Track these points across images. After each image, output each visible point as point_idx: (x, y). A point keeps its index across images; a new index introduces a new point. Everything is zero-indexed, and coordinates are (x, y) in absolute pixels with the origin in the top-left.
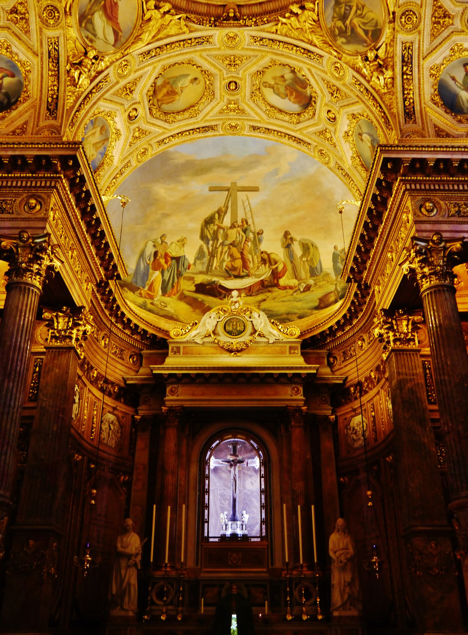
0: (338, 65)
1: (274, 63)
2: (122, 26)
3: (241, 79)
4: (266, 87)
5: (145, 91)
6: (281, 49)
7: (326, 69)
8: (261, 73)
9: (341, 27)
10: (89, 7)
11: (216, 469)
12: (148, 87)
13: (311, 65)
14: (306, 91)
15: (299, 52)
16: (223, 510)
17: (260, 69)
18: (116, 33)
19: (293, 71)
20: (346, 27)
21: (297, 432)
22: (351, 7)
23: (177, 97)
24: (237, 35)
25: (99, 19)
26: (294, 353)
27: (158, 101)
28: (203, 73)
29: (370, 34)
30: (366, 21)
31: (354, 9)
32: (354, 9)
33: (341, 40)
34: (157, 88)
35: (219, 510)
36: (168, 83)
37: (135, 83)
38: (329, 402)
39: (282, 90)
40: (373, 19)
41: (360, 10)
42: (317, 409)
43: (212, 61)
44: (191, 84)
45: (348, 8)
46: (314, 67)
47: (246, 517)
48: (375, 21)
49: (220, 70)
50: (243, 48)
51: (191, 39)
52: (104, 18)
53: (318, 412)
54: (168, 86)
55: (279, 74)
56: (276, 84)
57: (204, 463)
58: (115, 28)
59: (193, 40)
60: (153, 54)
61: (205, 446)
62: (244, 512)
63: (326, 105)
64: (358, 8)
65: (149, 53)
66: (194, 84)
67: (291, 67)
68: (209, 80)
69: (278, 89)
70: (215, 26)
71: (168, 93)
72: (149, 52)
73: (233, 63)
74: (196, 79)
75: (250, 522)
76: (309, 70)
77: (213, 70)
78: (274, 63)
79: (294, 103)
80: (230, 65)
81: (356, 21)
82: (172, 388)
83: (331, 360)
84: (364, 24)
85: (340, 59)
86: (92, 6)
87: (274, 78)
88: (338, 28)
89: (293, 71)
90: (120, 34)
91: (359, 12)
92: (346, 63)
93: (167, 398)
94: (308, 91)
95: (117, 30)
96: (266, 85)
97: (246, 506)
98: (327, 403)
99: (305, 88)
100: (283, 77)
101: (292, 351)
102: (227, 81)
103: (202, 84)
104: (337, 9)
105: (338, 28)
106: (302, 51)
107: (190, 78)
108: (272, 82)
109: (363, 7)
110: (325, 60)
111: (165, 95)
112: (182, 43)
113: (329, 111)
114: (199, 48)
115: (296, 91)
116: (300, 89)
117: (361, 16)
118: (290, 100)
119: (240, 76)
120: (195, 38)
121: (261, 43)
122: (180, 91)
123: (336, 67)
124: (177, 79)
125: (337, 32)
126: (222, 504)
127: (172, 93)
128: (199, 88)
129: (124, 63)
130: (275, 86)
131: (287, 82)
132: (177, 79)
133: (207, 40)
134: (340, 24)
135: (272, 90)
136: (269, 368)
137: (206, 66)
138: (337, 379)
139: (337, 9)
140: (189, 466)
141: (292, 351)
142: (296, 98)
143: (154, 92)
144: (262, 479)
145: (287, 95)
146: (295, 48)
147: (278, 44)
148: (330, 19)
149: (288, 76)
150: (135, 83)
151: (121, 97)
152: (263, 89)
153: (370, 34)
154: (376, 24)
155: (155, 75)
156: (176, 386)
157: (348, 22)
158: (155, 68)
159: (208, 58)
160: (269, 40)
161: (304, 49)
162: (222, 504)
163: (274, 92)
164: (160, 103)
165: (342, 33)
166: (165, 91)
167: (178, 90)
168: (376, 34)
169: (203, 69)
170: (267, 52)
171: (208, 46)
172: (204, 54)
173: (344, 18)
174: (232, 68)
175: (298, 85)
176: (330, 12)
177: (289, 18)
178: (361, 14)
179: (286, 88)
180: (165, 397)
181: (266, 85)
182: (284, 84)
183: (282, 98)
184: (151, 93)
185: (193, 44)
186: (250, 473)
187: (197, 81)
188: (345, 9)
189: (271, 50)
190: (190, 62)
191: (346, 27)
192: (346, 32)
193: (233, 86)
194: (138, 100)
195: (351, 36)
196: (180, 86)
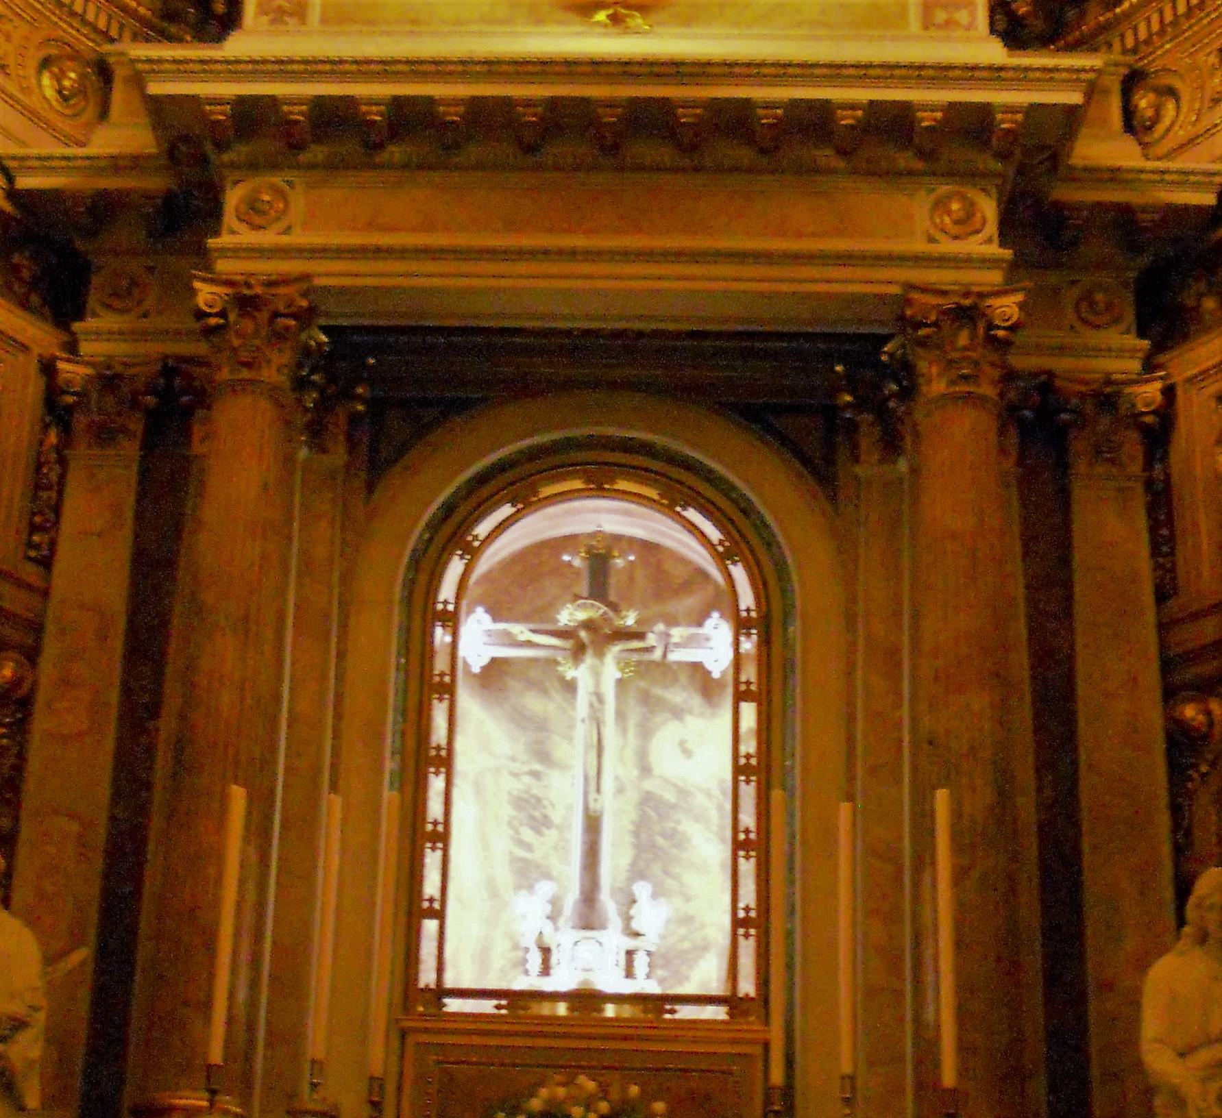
11: (494, 675)
16: (527, 873)
21: (956, 454)
26: (948, 24)
35: (505, 876)
38: (1130, 316)
42: (1062, 350)
47: (652, 916)
53: (1062, 364)
57: (423, 614)
61: (434, 526)
62: (642, 890)
75: (673, 935)
82: (257, 191)
83: (1144, 102)
93: (225, 240)
97: (655, 851)
98: (1117, 320)
101: (941, 16)
126: (520, 843)
136: (805, 71)
138: (1185, 179)
140: (344, 627)
141: (941, 16)
144: (749, 712)
156: (277, 180)
162: (520, 843)
180: (217, 233)
186: (677, 695)
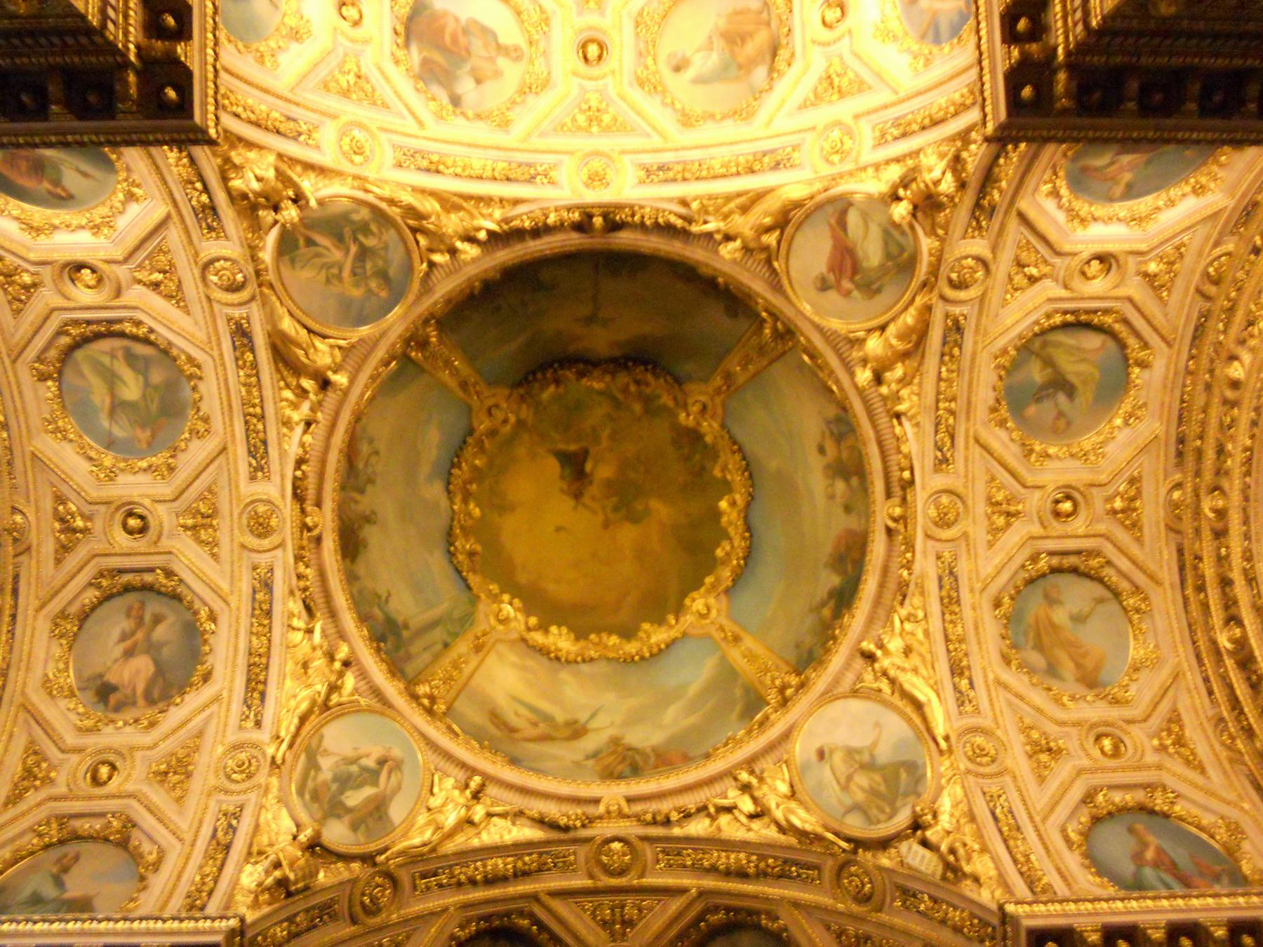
0: (358, 159)
1: (505, 124)
2: (827, 233)
3: (575, 74)
4: (517, 48)
5: (798, 65)
6: (489, 163)
7: (383, 137)
8: (526, 90)
9: (366, 236)
10: (887, 278)
12: (791, 75)
13: (416, 137)
14: (420, 52)
15: (450, 162)
17: (531, 99)
18: (842, 223)
19: (456, 101)
20: (355, 240)
22: (354, 274)
23: (722, 23)
24: (587, 186)
25: (872, 253)
27: (768, 24)
28: (659, 89)
29: (302, 242)
30: (317, 260)
31: (346, 273)
32: (346, 273)
33: (364, 214)
34: (768, 58)
36: (740, 67)
37: (816, 99)
39: (477, 46)
40: (302, 267)
41: (334, 276)
43: (639, 121)
44: (688, 54)
45: (358, 270)
46: (410, 136)
48: (298, 265)
49: (623, 98)
50: (571, 153)
51: (685, 179)
52: (860, 253)
54: (741, 59)
55: (489, 86)
56: (492, 60)
58: (842, 233)
59: (679, 176)
60: (766, 159)
63: (366, 42)
64: (339, 277)
65: (778, 164)
66: (680, 56)
67: (462, 113)
68: (647, 68)
69: (486, 46)
70: (632, 207)
71: (743, 41)
72: (777, 166)
73: (593, 118)
74: (677, 69)
76: (421, 124)
77: (636, 95)
78: (505, 124)
79: (445, 14)
80: (598, 110)
81: (337, 255)
84: (318, 255)
85: (356, 177)
86: (879, 279)
87: (498, 74)
88: (373, 234)
89: (456, 101)
90: (833, 221)
91: (335, 271)
92: (339, 174)
94: (416, 55)
95: (838, 230)
96: (513, 53)
99: (425, 62)
100: (479, 81)
102: (605, 68)
103: (663, 55)
104: (381, 263)
105: (373, 234)
106: (441, 167)
107: (690, 73)
108: (502, 62)
109: (328, 281)
110: (389, 157)
111: (751, 35)
112: (704, 173)
113: (356, 24)
114: (667, 157)
115: (441, 48)
116: (437, 57)
117: (329, 267)
118: (457, 20)
119: (576, 81)
120: (674, 180)
121: (532, 171)
122: (714, 39)
123: (361, 154)
124: (720, 75)
125: (374, 228)
127: (733, 38)
128: (670, 45)
129: (836, 158)
130: (493, 53)
131: (467, 67)
132: (720, 75)
133: (651, 173)
134: (370, 242)
135: (502, 40)
137: (652, 107)
139: (381, 263)
142: (442, 29)
143: (774, 54)
145: (466, 31)
146: (459, 170)
147: (496, 174)
148: (391, 246)
149: (466, 86)
150: (816, 99)
151: (857, 75)
152: (524, 46)
153: (302, 242)
154: (293, 261)
155: (772, 100)
157: (354, 249)
158: (768, 124)
159: (649, 130)
160: (516, 180)
161: (438, 172)
163: (495, 36)
164: (765, 15)
165: (364, 228)
166: (751, 48)
167: (719, 43)
168: (287, 244)
169: (658, 99)
170: (517, 150)
171: (648, 159)
172: (657, 142)
173: (364, 253)
174: (594, 104)
175: (440, 66)
176: (396, 256)
177: (479, 229)
178: (328, 268)
179: (468, 50)
181: (513, 53)
182: (474, 61)
183: (475, 22)
184: (783, 54)
185: (679, 168)
187: (674, 62)
188: (364, 268)
189: (510, 154)
190: (686, 120)
191: (355, 240)
192: (354, 232)
193: (593, 50)
194: (819, 49)
195: (337, 225)
196: (715, 57)
